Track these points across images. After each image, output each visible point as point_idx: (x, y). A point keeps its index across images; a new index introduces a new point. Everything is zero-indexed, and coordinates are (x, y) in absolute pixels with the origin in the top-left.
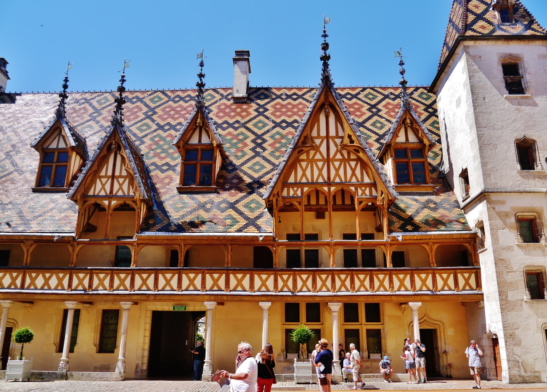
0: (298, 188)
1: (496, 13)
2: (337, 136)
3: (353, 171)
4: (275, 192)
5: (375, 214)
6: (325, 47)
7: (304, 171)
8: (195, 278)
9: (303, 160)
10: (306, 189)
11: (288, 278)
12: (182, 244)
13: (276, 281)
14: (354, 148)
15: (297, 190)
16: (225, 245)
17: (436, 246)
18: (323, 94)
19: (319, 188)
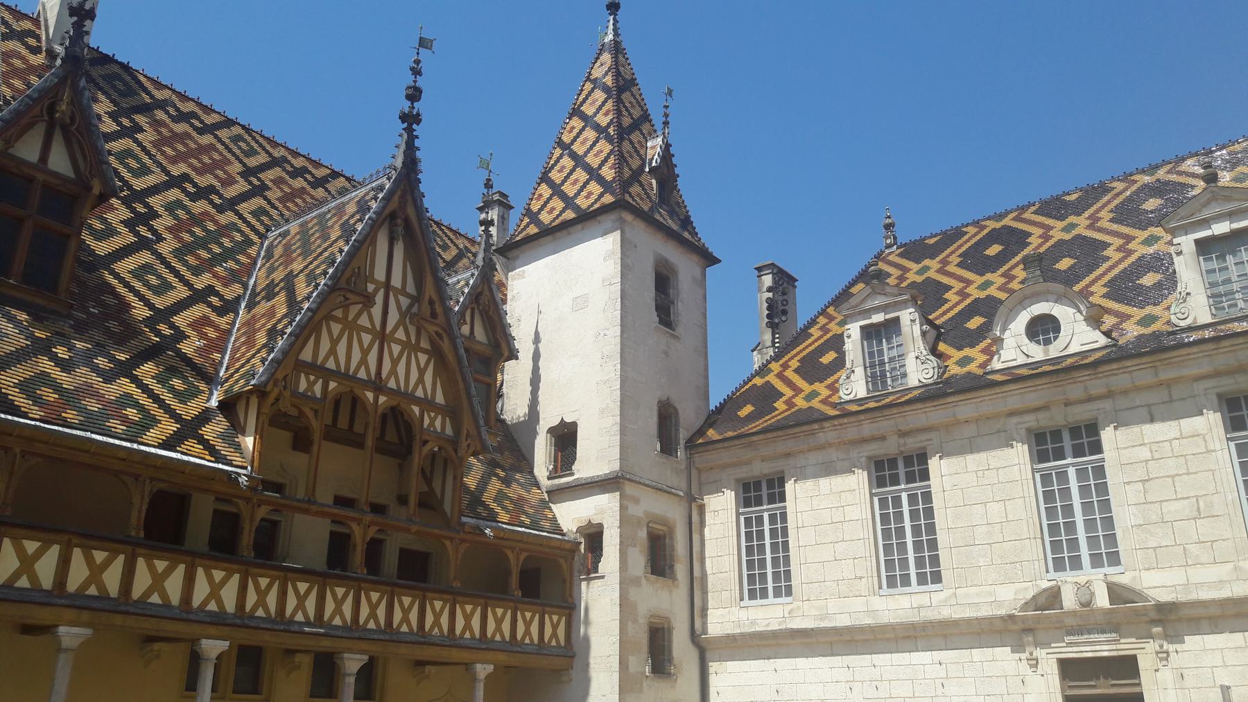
0: (317, 378)
1: (654, 181)
2: (403, 291)
3: (422, 372)
4: (280, 375)
5: (400, 466)
6: (414, 94)
7: (335, 342)
8: (39, 554)
9: (337, 320)
10: (332, 385)
11: (270, 586)
12: (18, 450)
13: (243, 589)
14: (436, 329)
15: (315, 382)
16: (137, 477)
17: (522, 558)
18: (399, 193)
19: (357, 391)
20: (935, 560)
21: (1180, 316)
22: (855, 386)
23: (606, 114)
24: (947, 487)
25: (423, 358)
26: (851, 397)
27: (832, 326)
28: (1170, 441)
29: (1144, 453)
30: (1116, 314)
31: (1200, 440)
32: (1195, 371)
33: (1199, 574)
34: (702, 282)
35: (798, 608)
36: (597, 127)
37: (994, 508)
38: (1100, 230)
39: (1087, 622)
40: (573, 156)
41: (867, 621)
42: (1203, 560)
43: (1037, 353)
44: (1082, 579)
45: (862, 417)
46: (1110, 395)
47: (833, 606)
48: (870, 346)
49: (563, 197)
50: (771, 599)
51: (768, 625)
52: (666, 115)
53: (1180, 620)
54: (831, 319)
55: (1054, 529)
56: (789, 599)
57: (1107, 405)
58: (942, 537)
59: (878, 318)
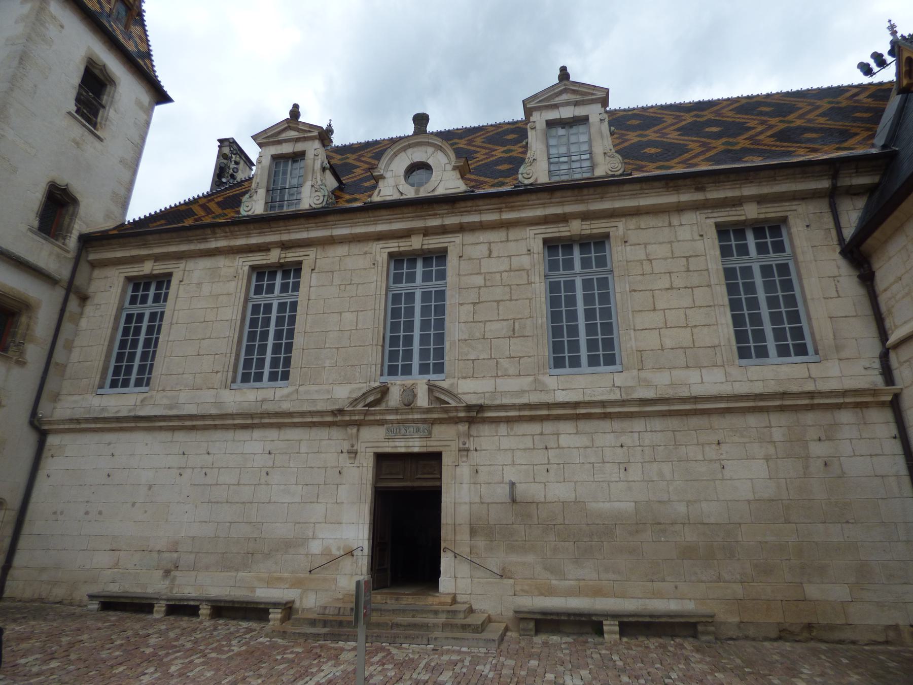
20: (287, 361)
21: (525, 176)
24: (313, 297)
28: (501, 273)
29: (479, 280)
31: (524, 274)
34: (149, 112)
35: (151, 397)
37: (349, 317)
41: (214, 411)
42: (511, 372)
43: (410, 193)
46: (461, 229)
47: (183, 397)
50: (131, 388)
51: (118, 412)
53: (485, 421)
55: (394, 341)
56: (147, 388)
57: (457, 239)
58: (298, 340)
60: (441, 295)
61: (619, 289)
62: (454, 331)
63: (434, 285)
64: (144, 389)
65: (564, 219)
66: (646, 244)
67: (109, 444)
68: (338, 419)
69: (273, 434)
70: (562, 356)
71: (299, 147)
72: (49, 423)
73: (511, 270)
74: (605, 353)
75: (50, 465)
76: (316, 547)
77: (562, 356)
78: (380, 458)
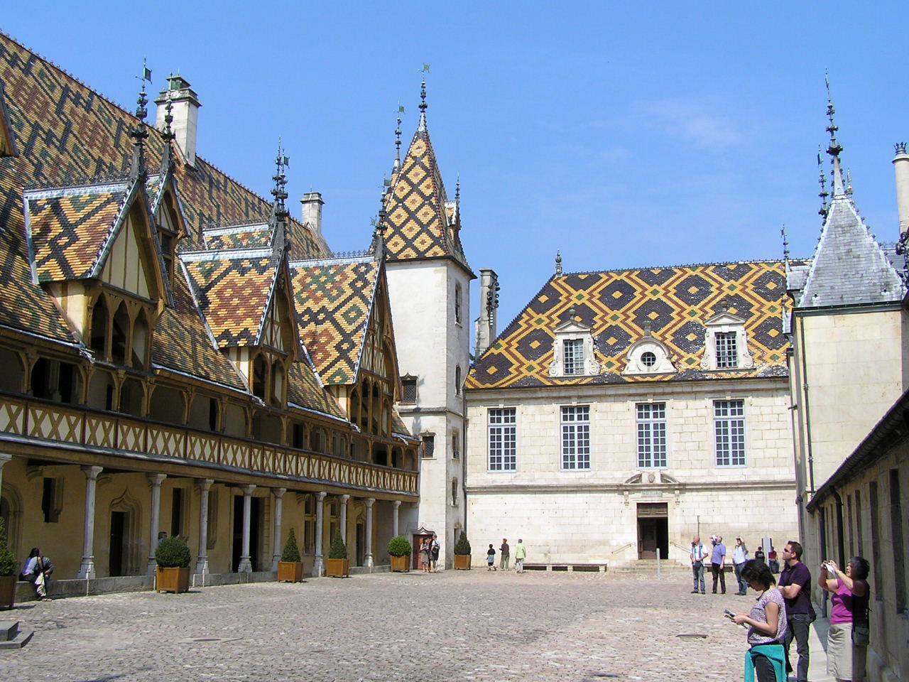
22: (558, 370)
23: (428, 187)
25: (381, 354)
26: (555, 375)
27: (531, 322)
29: (682, 421)
30: (678, 354)
32: (707, 389)
33: (695, 473)
35: (520, 475)
36: (421, 194)
37: (618, 437)
38: (670, 299)
39: (651, 487)
40: (406, 209)
43: (644, 369)
44: (651, 471)
45: (562, 388)
46: (672, 393)
47: (537, 475)
48: (566, 349)
49: (403, 237)
52: (458, 190)
54: (532, 318)
55: (641, 449)
59: (573, 337)
60: (663, 426)
61: (746, 427)
62: (671, 445)
63: (659, 420)
64: (510, 471)
65: (723, 391)
66: (761, 406)
67: (502, 498)
68: (619, 489)
69: (588, 495)
70: (722, 460)
71: (579, 336)
72: (469, 488)
73: (697, 416)
74: (740, 459)
75: (470, 508)
76: (614, 543)
77: (722, 460)
78: (639, 505)
